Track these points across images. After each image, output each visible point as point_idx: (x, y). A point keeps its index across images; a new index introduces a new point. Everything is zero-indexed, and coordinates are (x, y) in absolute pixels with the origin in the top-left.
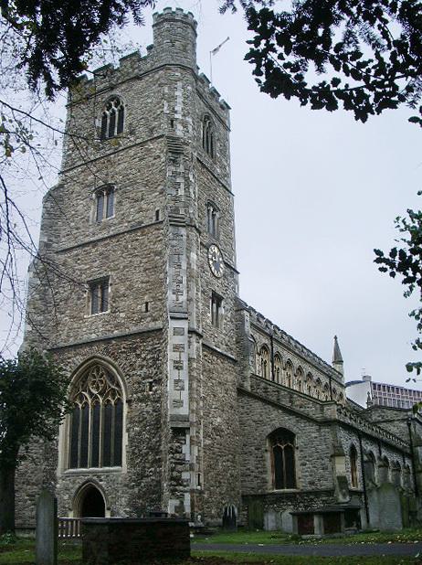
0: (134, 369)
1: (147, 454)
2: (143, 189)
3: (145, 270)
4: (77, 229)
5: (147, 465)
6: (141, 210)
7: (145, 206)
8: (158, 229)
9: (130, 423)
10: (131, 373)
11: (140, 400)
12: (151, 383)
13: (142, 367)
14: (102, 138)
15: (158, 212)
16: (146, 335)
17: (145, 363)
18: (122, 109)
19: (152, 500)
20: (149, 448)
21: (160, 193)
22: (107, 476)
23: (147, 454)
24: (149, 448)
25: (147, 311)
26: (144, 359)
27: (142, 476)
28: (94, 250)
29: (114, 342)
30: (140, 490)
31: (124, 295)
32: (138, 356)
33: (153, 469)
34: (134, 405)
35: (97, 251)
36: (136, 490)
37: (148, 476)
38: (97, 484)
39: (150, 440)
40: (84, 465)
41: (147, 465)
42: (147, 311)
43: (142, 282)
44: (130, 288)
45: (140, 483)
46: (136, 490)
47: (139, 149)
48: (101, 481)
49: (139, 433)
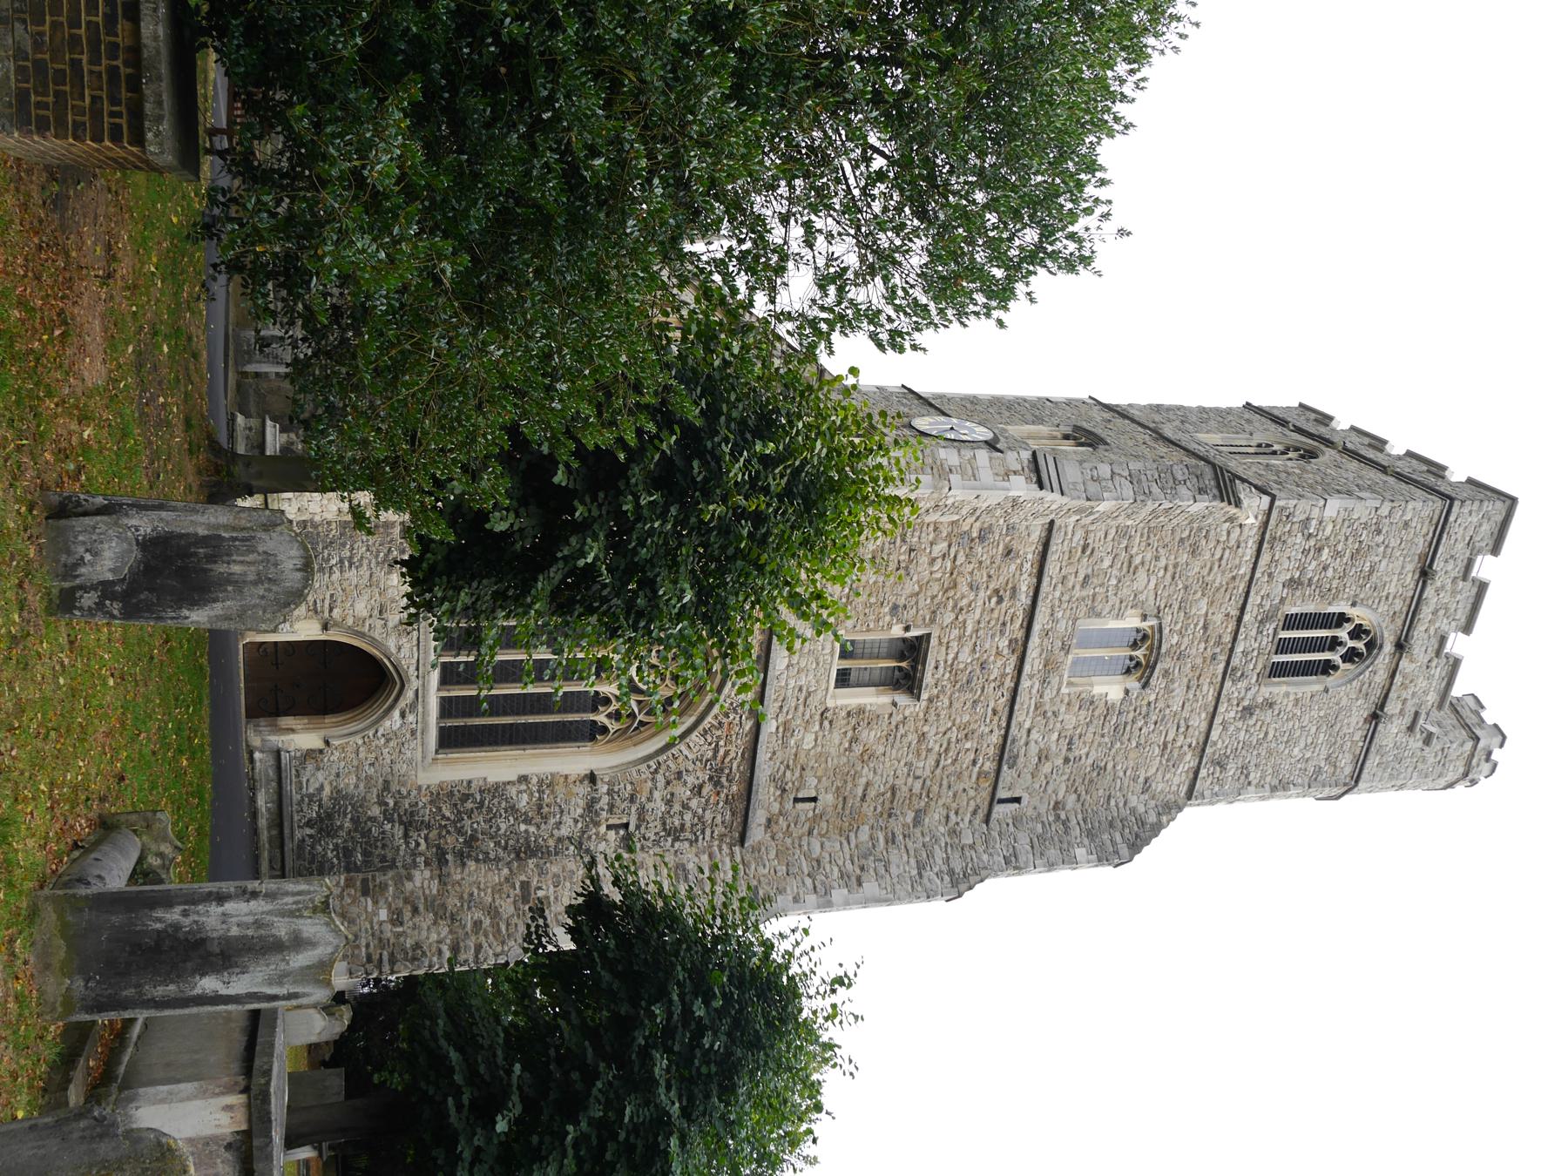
0: (668, 783)
1: (460, 832)
2: (1090, 761)
3: (893, 789)
4: (1087, 577)
5: (433, 834)
6: (1043, 756)
7: (1047, 768)
8: (974, 813)
9: (541, 782)
10: (659, 777)
11: (591, 805)
12: (626, 826)
13: (669, 803)
14: (1292, 622)
15: (1017, 800)
16: (742, 806)
17: (677, 807)
18: (1327, 668)
19: (348, 853)
20: (473, 838)
21: (1057, 803)
22: (413, 733)
23: (460, 832)
24: (473, 838)
25: (796, 800)
26: (685, 806)
27: (410, 823)
28: (1004, 643)
29: (748, 725)
30: (373, 819)
31: (854, 740)
32: (698, 790)
33: (423, 847)
34: (583, 789)
35: (998, 653)
36: (376, 811)
37: (406, 836)
38: (392, 707)
39: (492, 838)
40: (445, 681)
41: (433, 834)
42: (796, 800)
43: (868, 784)
44: (867, 756)
45: (391, 821)
46: (376, 811)
47: (1195, 737)
48: (403, 715)
49: (512, 809)
